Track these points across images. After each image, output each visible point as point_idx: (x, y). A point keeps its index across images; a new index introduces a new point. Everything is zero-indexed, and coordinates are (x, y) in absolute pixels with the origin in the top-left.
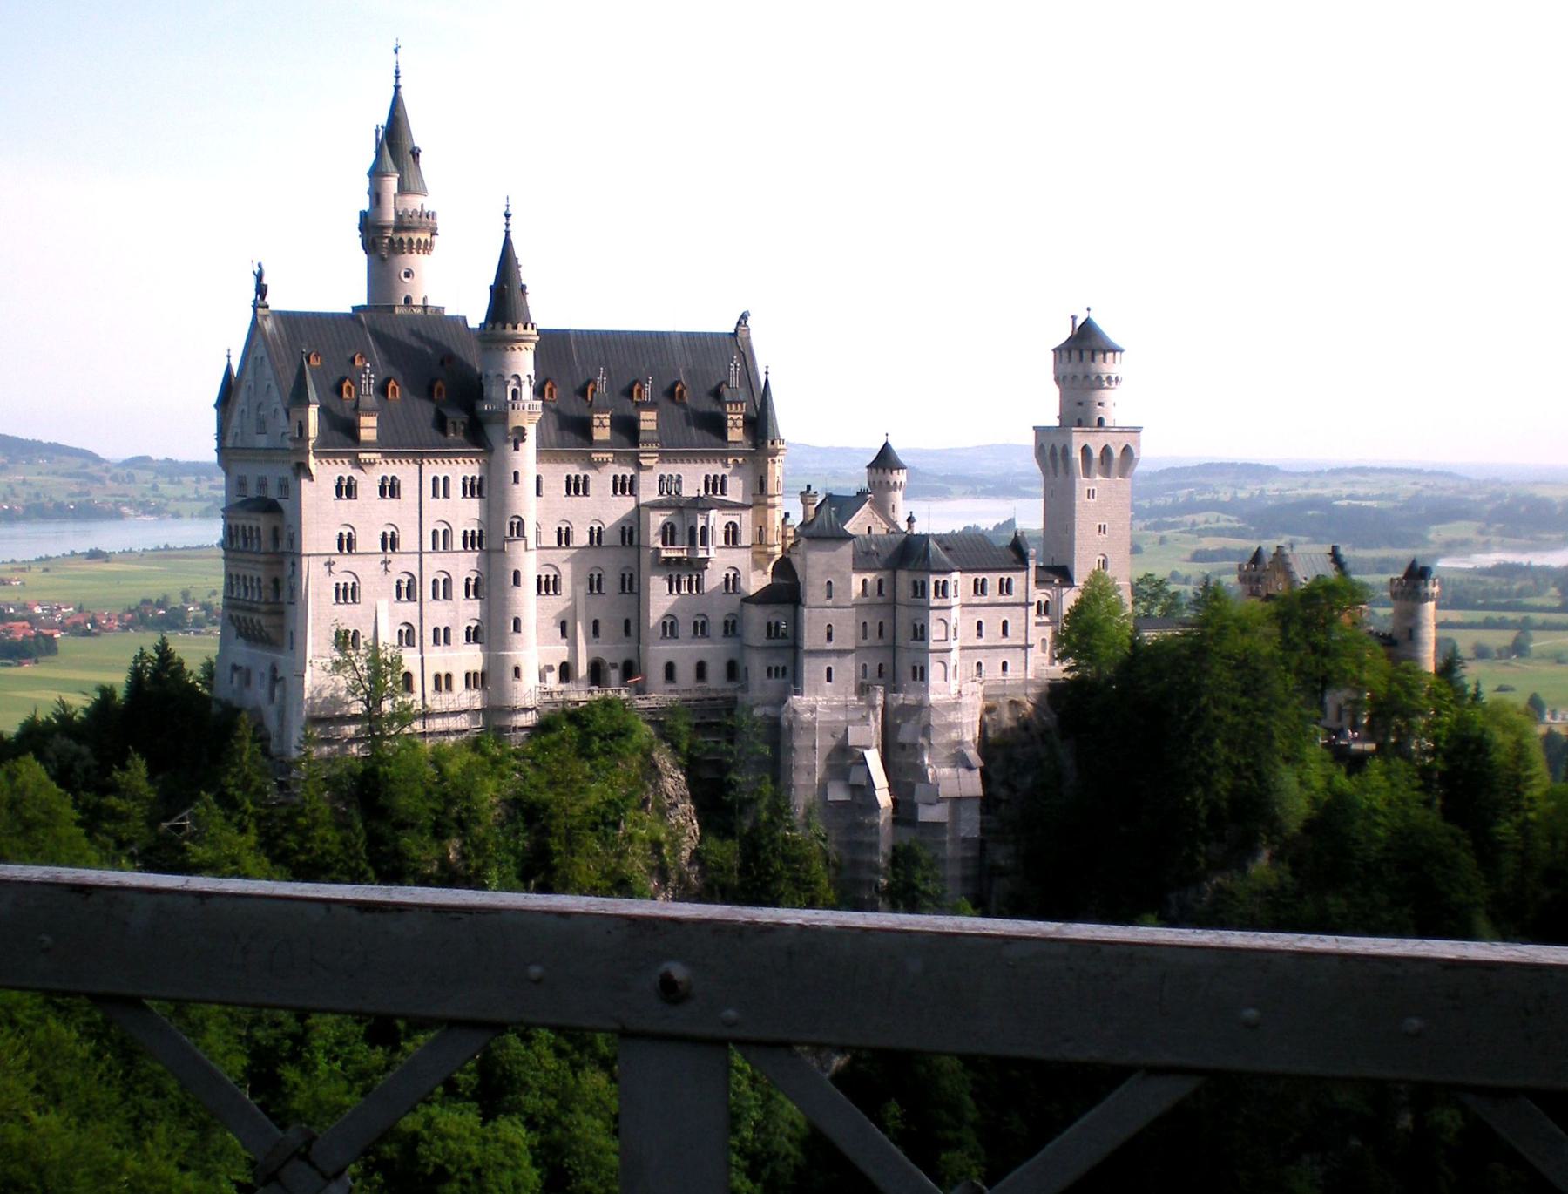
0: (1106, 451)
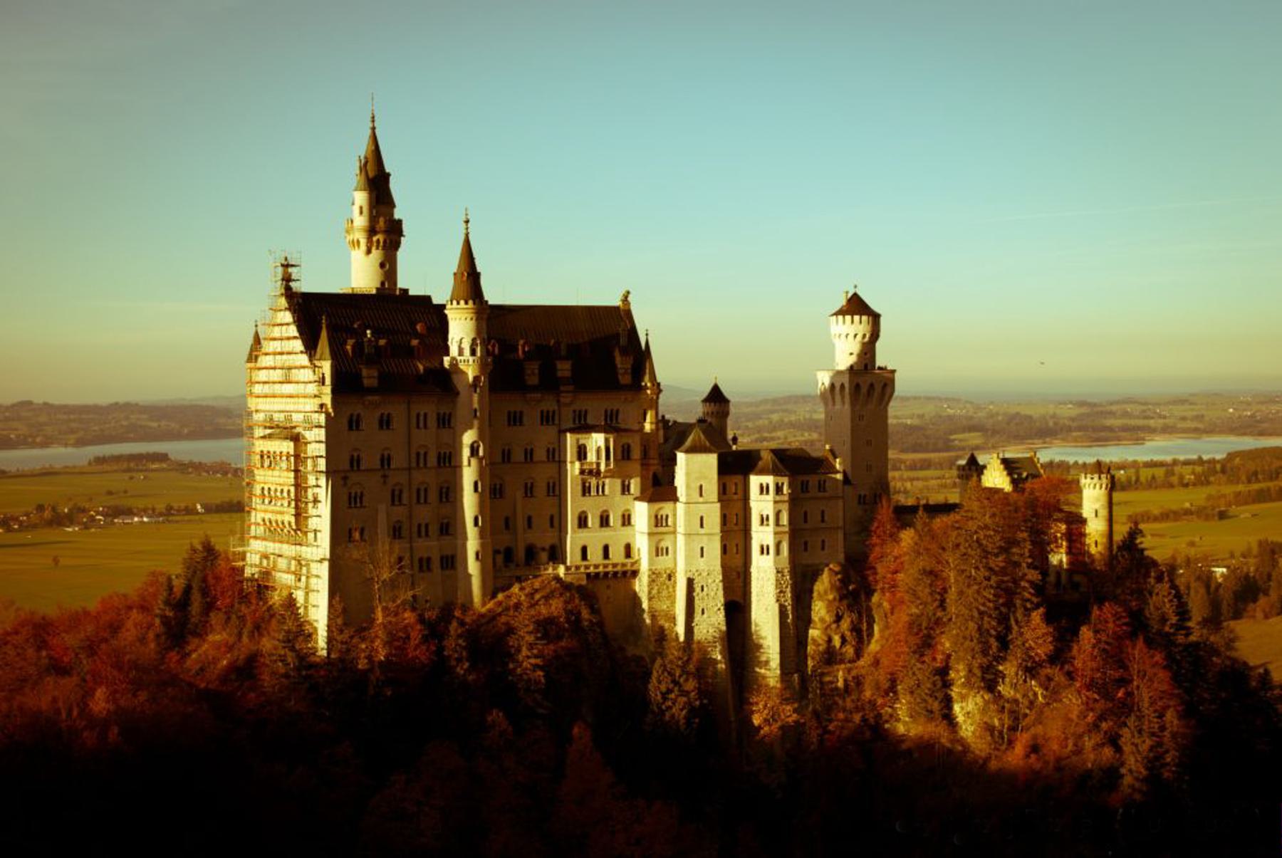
0: (872, 385)
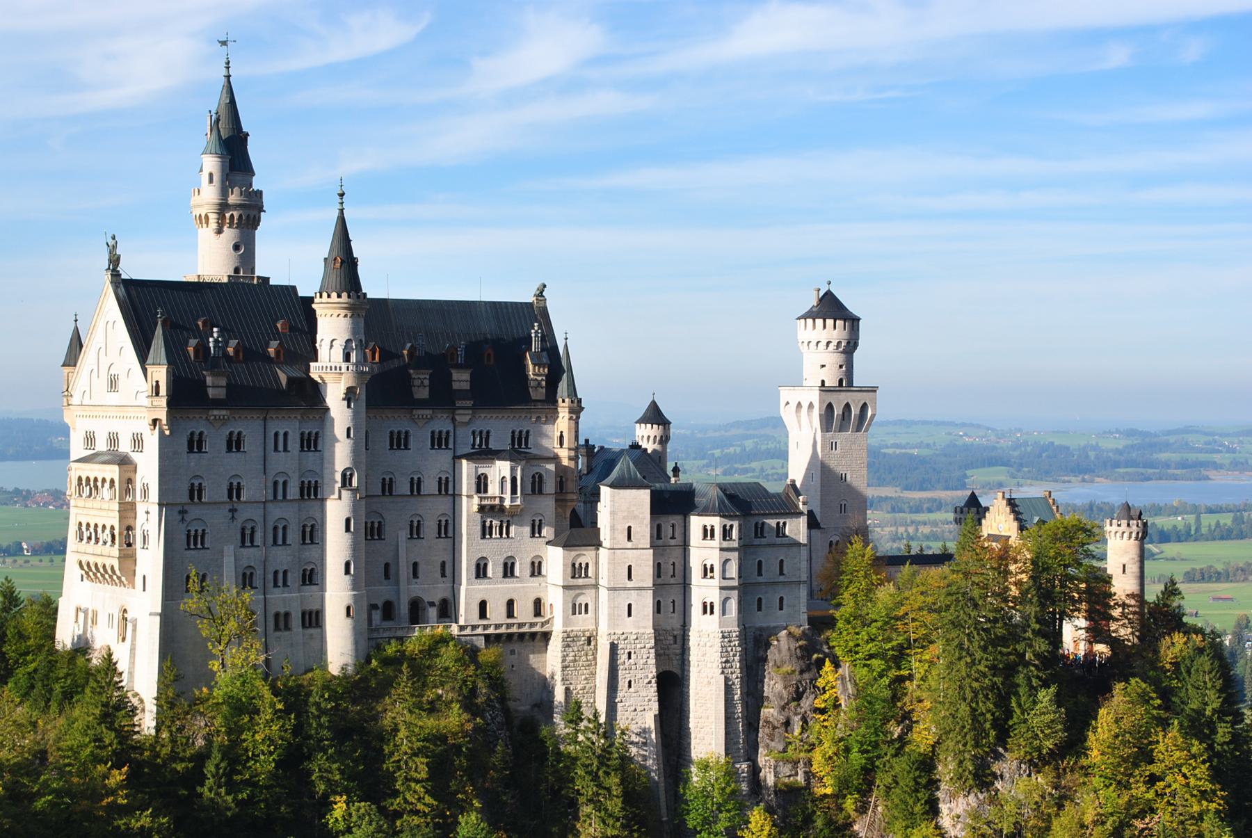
0: (847, 406)
